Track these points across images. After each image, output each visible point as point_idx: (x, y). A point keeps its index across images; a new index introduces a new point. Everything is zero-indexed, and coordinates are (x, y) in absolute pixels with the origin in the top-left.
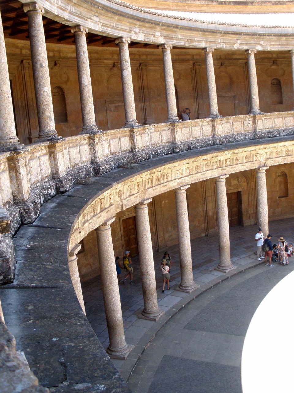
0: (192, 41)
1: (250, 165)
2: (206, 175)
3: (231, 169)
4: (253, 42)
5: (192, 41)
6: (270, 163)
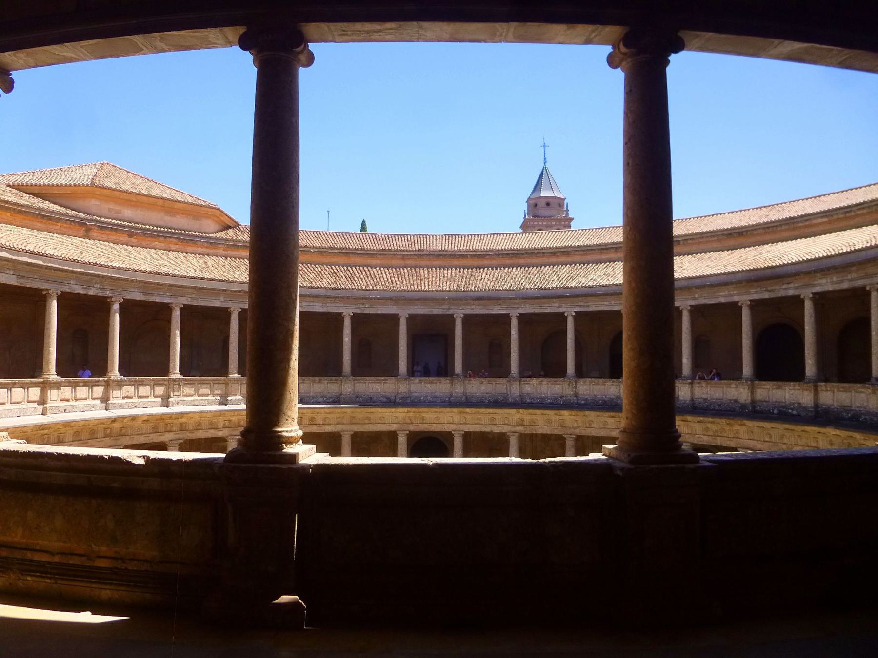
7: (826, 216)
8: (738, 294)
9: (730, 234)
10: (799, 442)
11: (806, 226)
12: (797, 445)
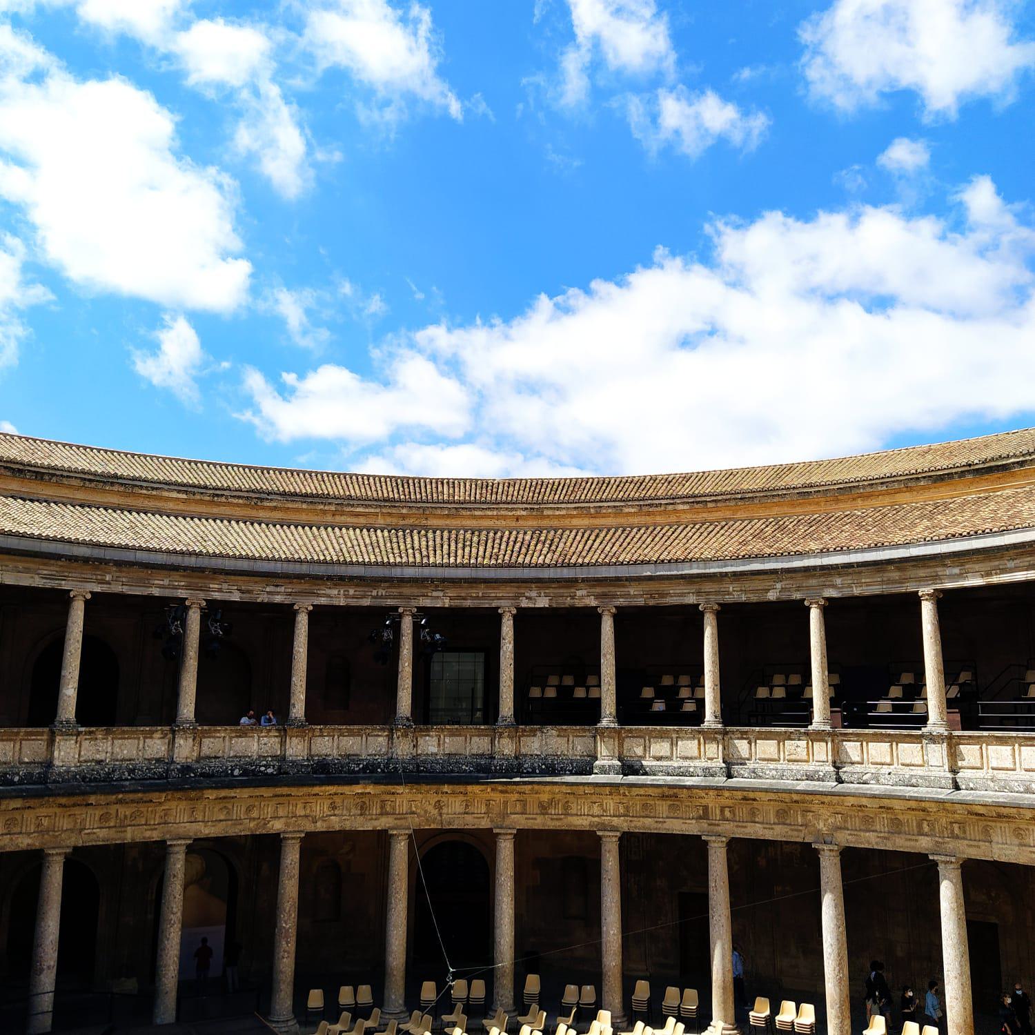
0: (662, 595)
1: (787, 832)
2: (665, 826)
3: (735, 829)
4: (813, 582)
5: (662, 595)
6: (846, 839)
7: (186, 492)
8: (187, 587)
9: (20, 471)
10: (281, 813)
11: (149, 497)
12: (276, 818)
